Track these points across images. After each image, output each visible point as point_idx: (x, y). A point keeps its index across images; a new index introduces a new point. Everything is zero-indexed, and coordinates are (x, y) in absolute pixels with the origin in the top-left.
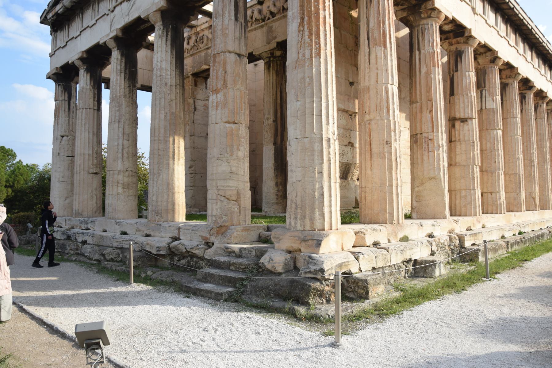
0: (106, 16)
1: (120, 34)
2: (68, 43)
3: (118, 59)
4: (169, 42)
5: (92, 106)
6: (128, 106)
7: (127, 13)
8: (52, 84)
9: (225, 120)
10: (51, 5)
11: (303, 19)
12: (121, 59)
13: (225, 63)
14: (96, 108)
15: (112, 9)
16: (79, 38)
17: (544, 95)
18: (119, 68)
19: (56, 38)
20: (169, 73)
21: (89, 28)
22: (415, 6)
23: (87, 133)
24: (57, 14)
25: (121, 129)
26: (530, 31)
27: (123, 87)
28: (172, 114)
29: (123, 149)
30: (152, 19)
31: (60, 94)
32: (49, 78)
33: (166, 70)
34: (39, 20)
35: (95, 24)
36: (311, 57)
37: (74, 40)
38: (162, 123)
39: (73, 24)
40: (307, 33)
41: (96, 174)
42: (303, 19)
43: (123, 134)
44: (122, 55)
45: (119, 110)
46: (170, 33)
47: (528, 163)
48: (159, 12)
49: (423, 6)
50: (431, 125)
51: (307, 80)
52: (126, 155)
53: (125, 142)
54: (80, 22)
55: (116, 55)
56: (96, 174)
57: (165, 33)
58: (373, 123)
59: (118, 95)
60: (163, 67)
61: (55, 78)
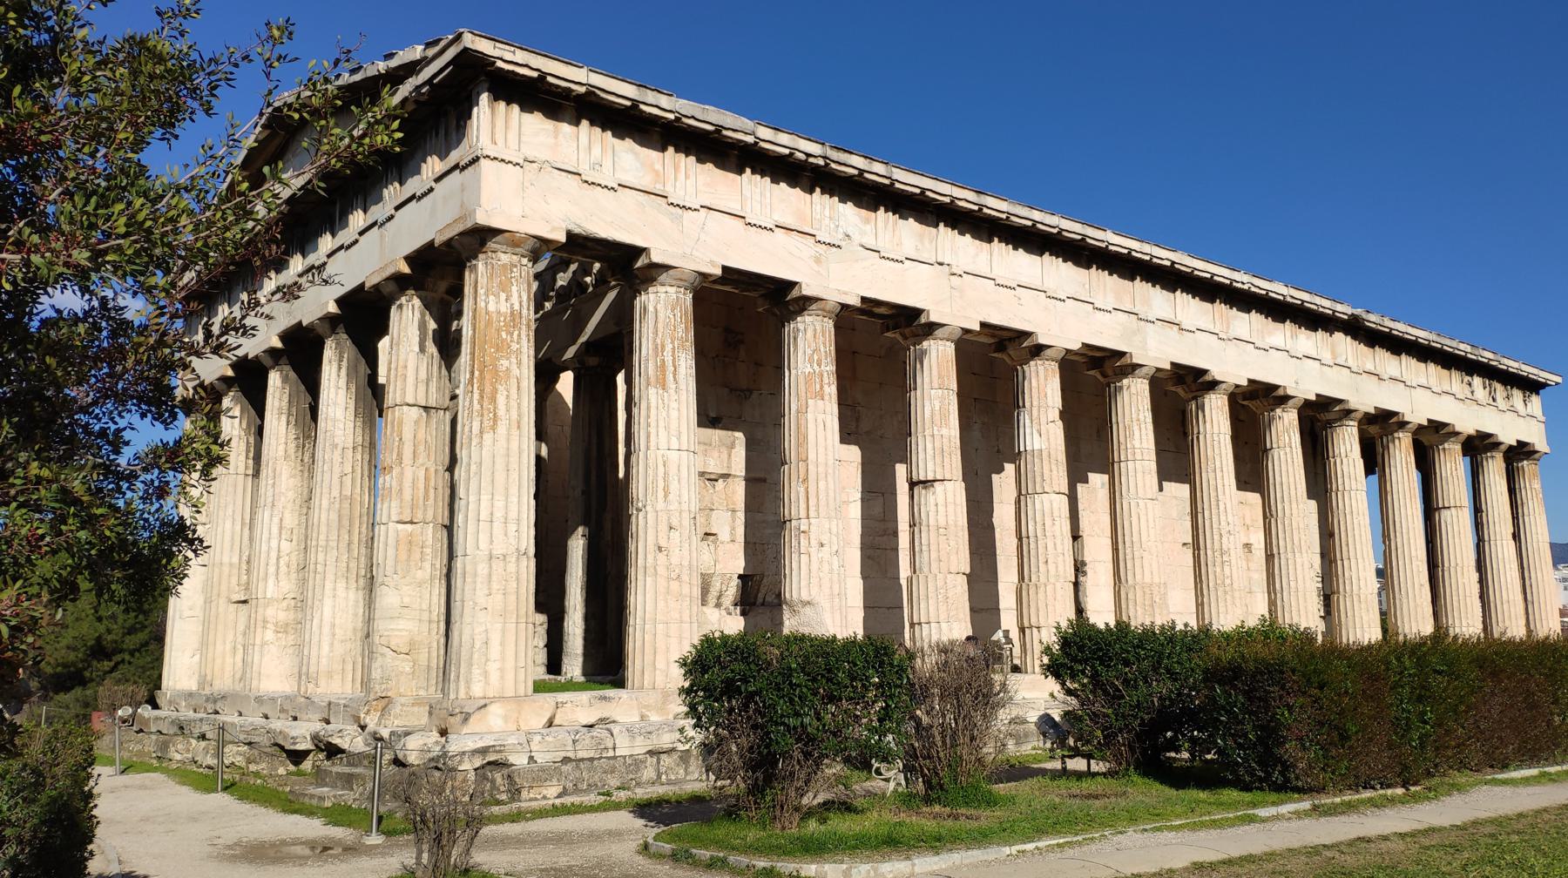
4: (344, 372)
9: (394, 518)
11: (472, 373)
13: (401, 423)
14: (250, 472)
25: (276, 520)
28: (342, 498)
29: (278, 558)
30: (320, 330)
40: (476, 396)
42: (472, 373)
43: (281, 528)
50: (803, 506)
51: (473, 467)
52: (283, 568)
53: (285, 545)
55: (274, 379)
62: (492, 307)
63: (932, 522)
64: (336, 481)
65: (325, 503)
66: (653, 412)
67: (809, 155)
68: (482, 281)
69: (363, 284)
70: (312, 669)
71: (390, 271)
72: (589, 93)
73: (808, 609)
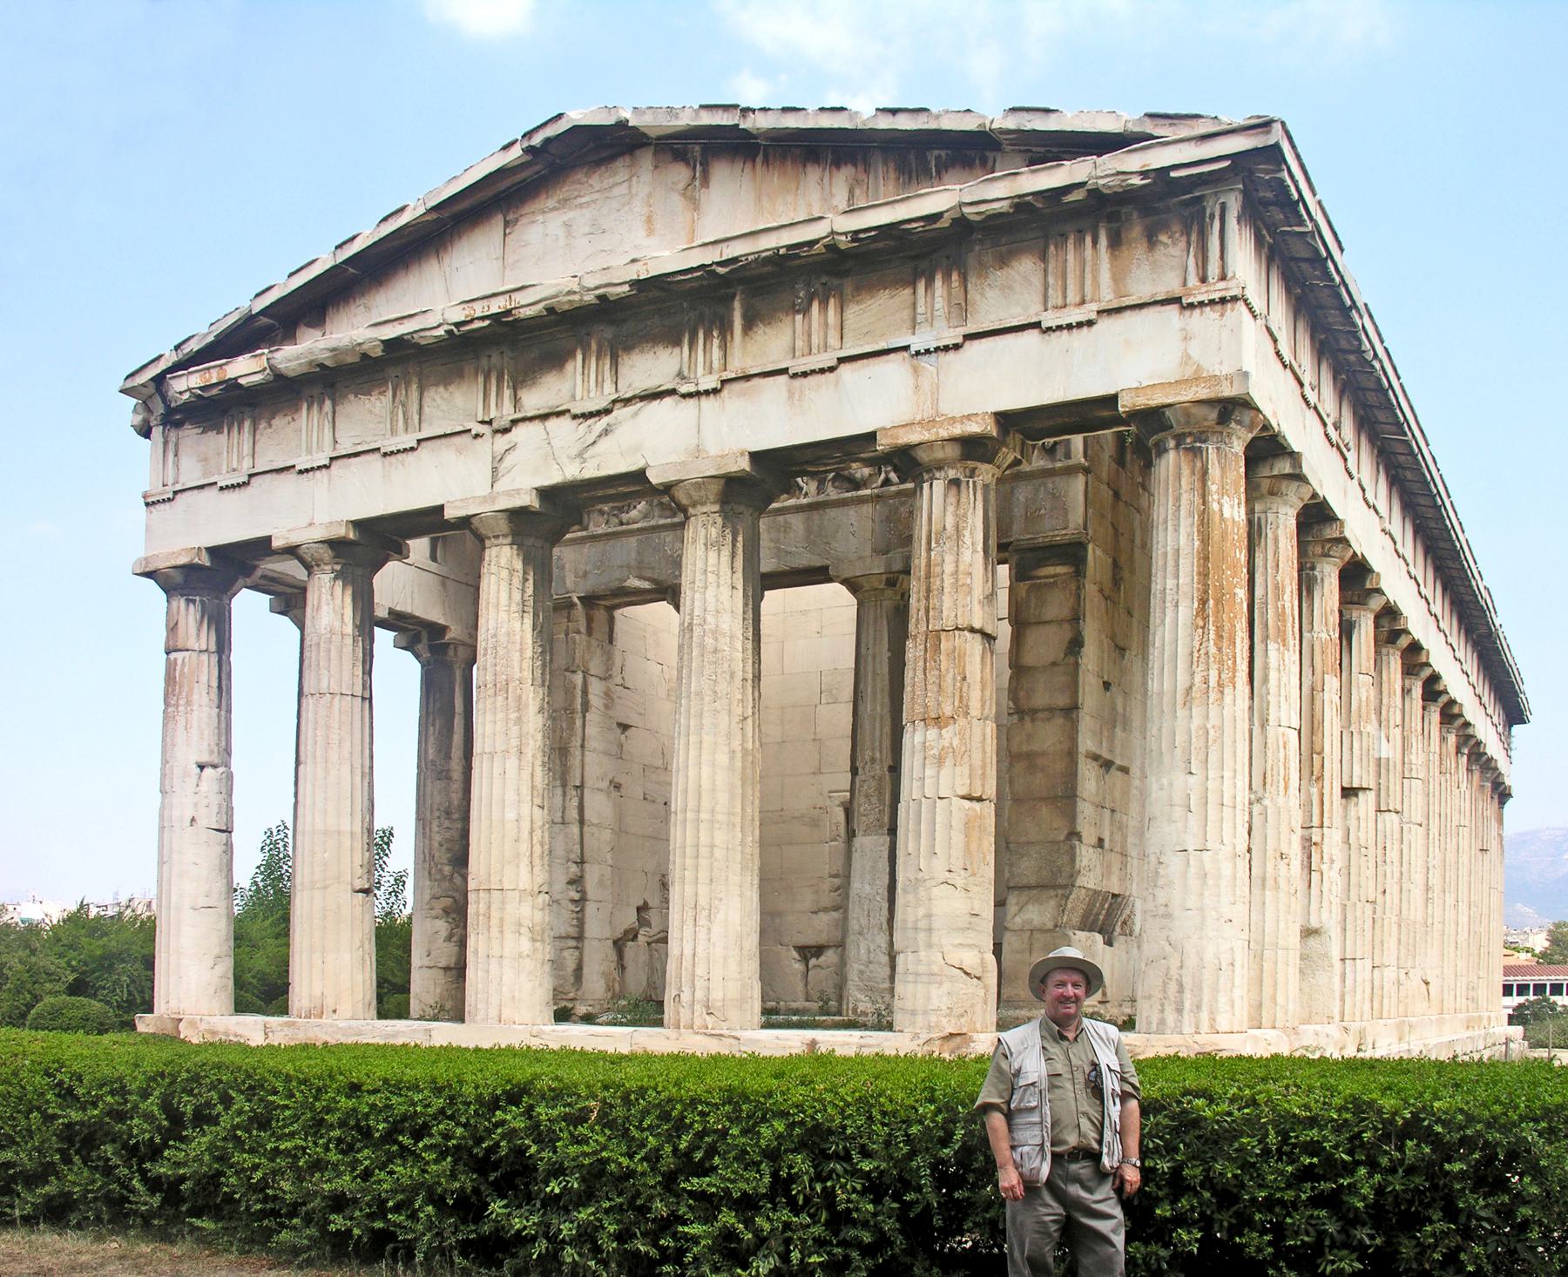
0: (466, 438)
1: (536, 505)
2: (253, 480)
3: (512, 571)
6: (541, 710)
7: (575, 452)
10: (194, 346)
12: (525, 573)
15: (505, 423)
18: (517, 596)
19: (177, 445)
20: (739, 646)
21: (377, 456)
23: (346, 770)
24: (232, 385)
27: (529, 653)
33: (731, 637)
34: (120, 383)
35: (412, 449)
37: (291, 477)
38: (721, 778)
39: (277, 422)
44: (525, 563)
45: (519, 718)
46: (740, 539)
48: (722, 481)
57: (729, 537)
59: (517, 676)
60: (725, 627)
64: (736, 727)
65: (722, 758)
69: (871, 437)
71: (974, 428)
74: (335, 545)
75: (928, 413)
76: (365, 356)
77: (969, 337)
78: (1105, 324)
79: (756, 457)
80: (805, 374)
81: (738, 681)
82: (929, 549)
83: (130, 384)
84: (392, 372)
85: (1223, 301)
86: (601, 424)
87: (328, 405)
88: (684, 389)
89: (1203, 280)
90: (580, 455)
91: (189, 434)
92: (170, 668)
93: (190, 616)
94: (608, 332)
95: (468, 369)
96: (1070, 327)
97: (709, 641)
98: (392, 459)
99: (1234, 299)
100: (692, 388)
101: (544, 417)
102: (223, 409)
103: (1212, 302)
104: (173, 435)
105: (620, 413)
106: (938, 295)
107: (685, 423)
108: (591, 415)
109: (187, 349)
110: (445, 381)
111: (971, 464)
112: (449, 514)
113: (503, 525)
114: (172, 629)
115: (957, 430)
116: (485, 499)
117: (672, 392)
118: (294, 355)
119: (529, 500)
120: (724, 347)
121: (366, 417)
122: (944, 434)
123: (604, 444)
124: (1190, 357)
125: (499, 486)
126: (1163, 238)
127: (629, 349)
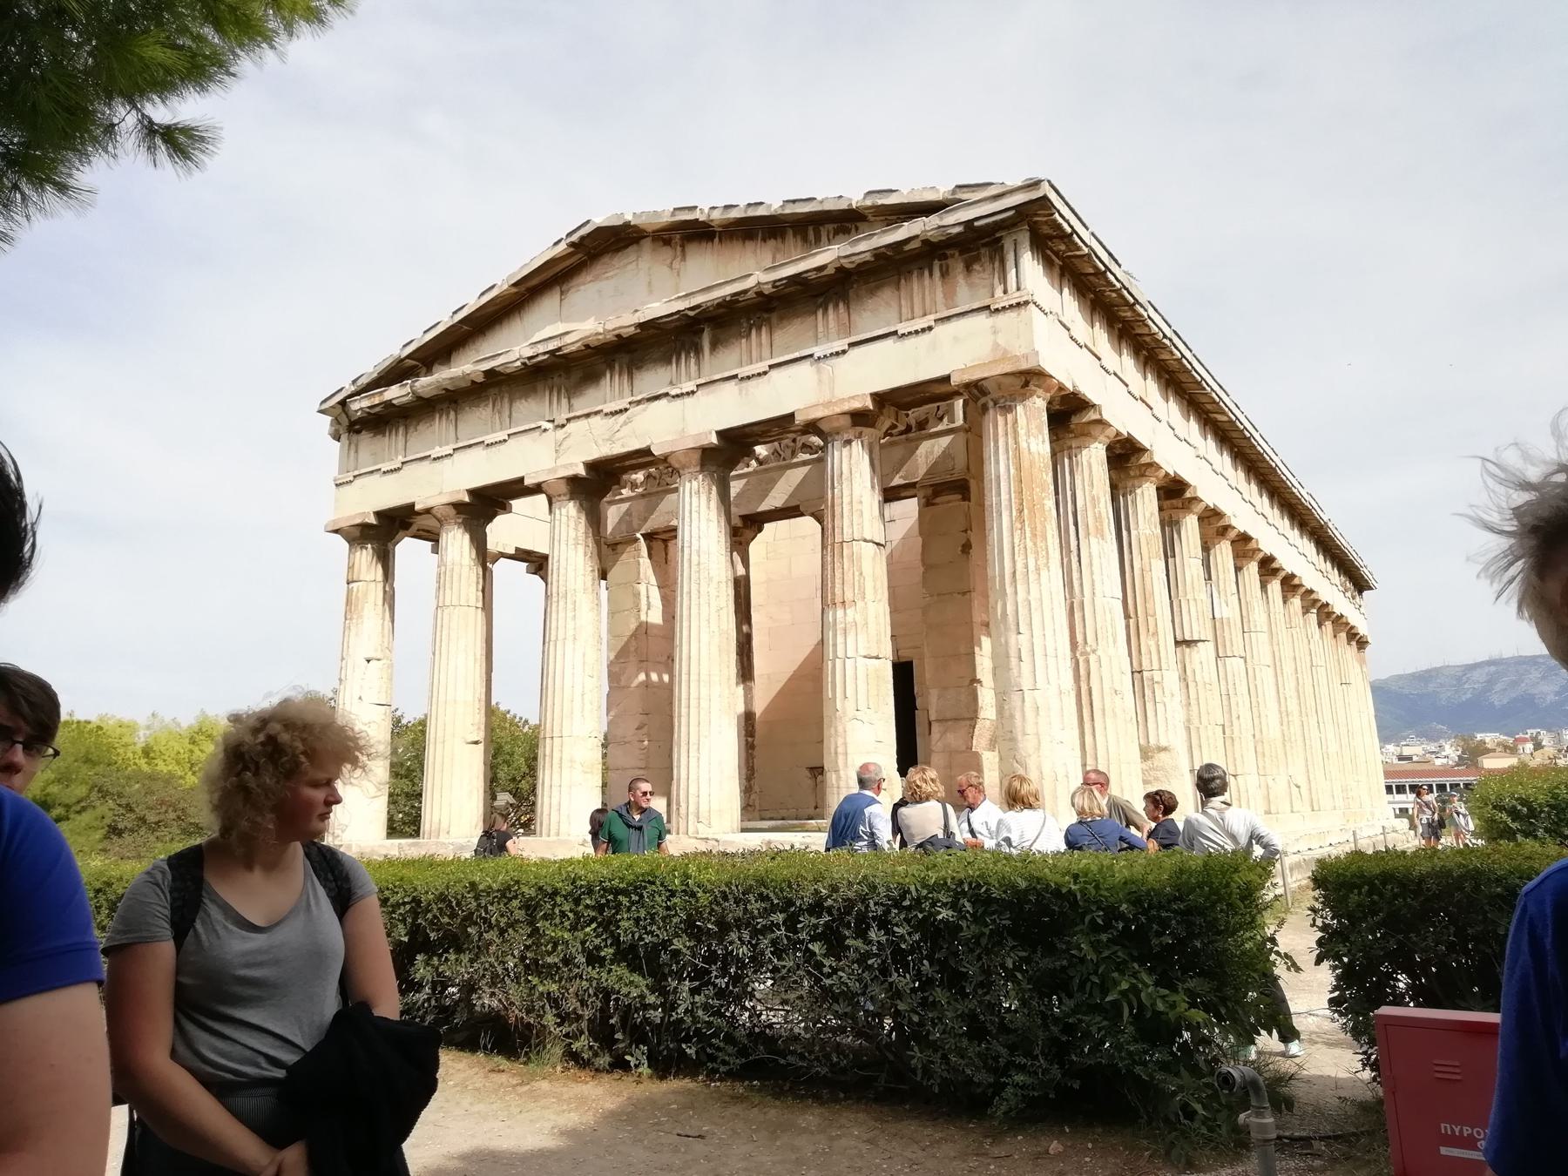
0: (537, 433)
1: (582, 471)
5: (472, 602)
8: (341, 543)
10: (364, 381)
16: (447, 461)
17: (1296, 581)
18: (572, 534)
22: (1120, 455)
24: (388, 404)
26: (1273, 470)
31: (364, 567)
32: (336, 531)
34: (317, 407)
36: (1038, 569)
40: (1028, 534)
41: (476, 743)
42: (1021, 511)
47: (1284, 715)
49: (1133, 459)
54: (452, 428)
56: (476, 743)
58: (1092, 658)
61: (357, 533)
62: (1033, 448)
63: (1198, 678)
66: (1096, 562)
67: (1165, 336)
68: (1022, 421)
69: (792, 415)
70: (703, 808)
71: (857, 405)
72: (1088, 255)
73: (1163, 755)
74: (458, 506)
75: (827, 398)
76: (473, 382)
77: (852, 345)
78: (940, 330)
79: (721, 434)
80: (748, 378)
81: (714, 585)
82: (833, 487)
83: (325, 406)
84: (492, 391)
85: (1018, 304)
86: (622, 418)
87: (452, 414)
88: (673, 393)
89: (1005, 292)
90: (611, 440)
91: (365, 437)
92: (349, 592)
93: (365, 556)
94: (626, 358)
95: (540, 386)
96: (917, 332)
97: (695, 558)
98: (494, 449)
99: (1026, 303)
100: (678, 391)
101: (588, 416)
102: (382, 421)
103: (1011, 306)
104: (355, 437)
105: (633, 410)
106: (832, 318)
107: (676, 414)
108: (616, 413)
109: (359, 383)
110: (526, 396)
111: (859, 429)
112: (527, 482)
113: (563, 488)
114: (351, 568)
115: (846, 407)
116: (550, 471)
117: (667, 394)
118: (426, 383)
119: (581, 471)
120: (698, 364)
121: (476, 421)
122: (838, 410)
123: (625, 430)
124: (996, 346)
125: (560, 462)
126: (977, 267)
127: (639, 368)
